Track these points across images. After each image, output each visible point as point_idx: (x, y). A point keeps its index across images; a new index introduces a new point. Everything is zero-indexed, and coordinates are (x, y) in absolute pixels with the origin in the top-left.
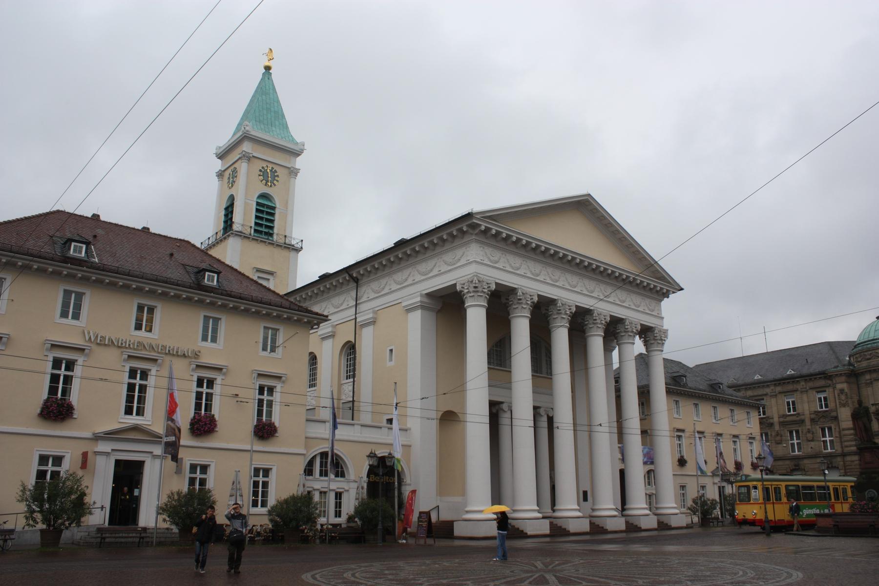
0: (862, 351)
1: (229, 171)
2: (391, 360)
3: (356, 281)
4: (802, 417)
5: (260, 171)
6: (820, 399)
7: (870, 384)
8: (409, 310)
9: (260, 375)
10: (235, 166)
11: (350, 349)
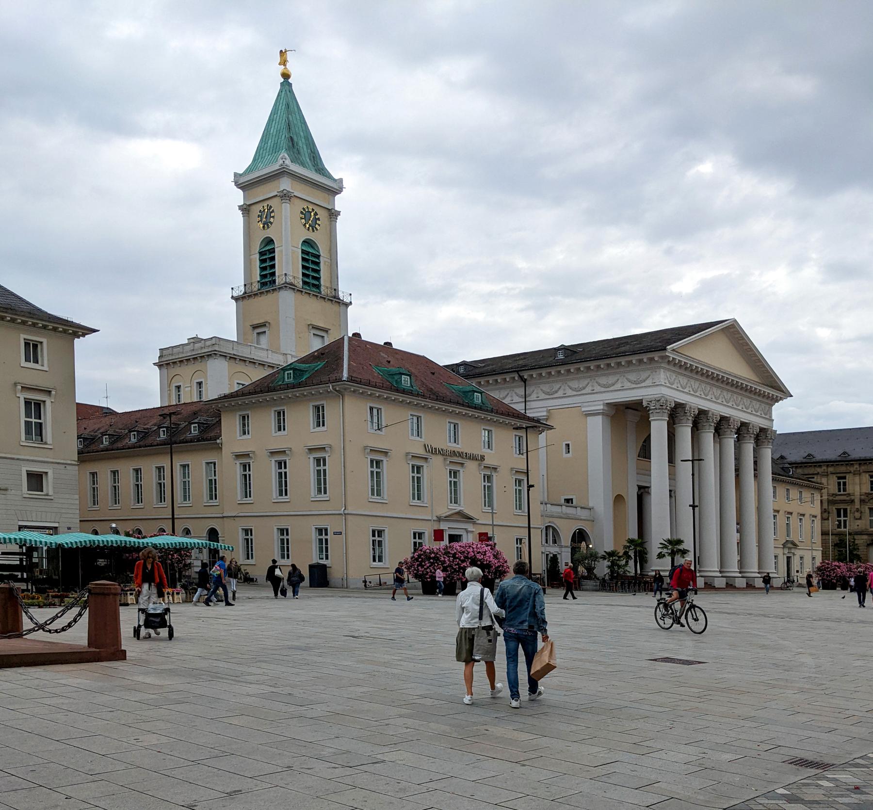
1: (259, 207)
3: (525, 381)
4: (852, 497)
5: (302, 213)
8: (589, 414)
10: (270, 203)
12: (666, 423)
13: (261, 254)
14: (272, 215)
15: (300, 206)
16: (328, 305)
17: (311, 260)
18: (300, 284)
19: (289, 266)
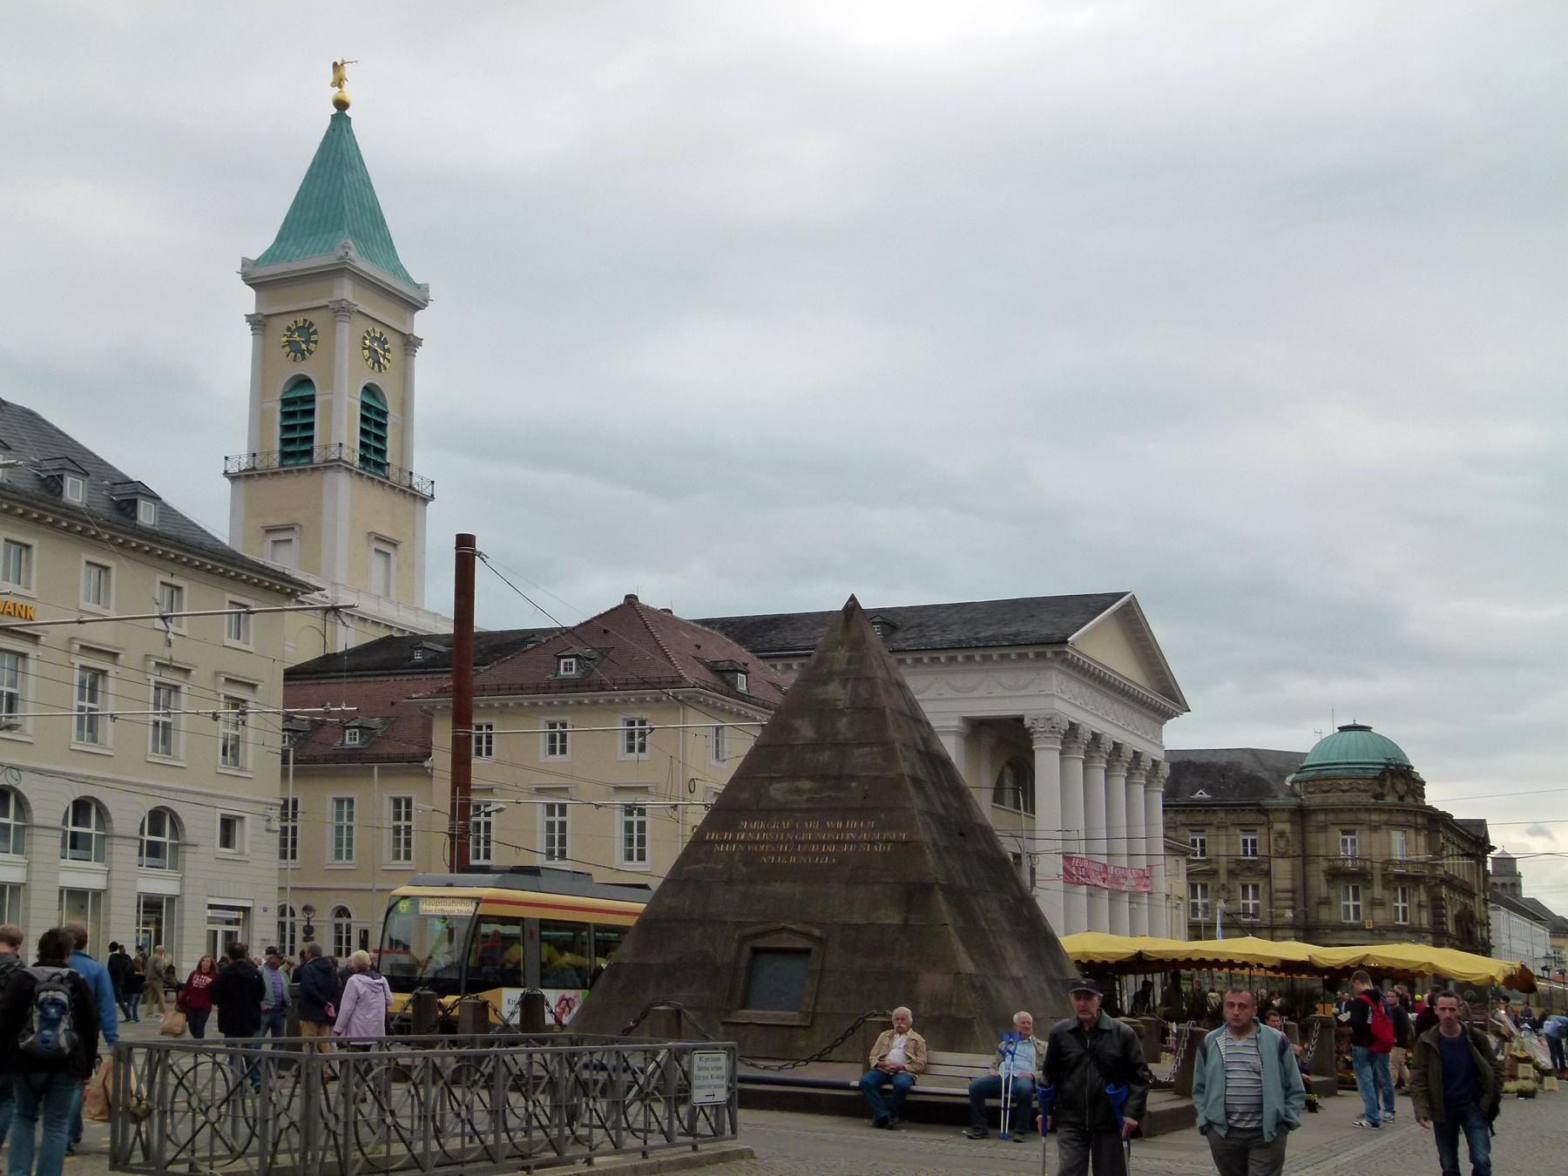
0: (1312, 780)
4: (1214, 866)
6: (1245, 842)
7: (1323, 828)
10: (311, 317)
13: (286, 402)
14: (313, 338)
16: (398, 499)
17: (374, 420)
19: (339, 428)
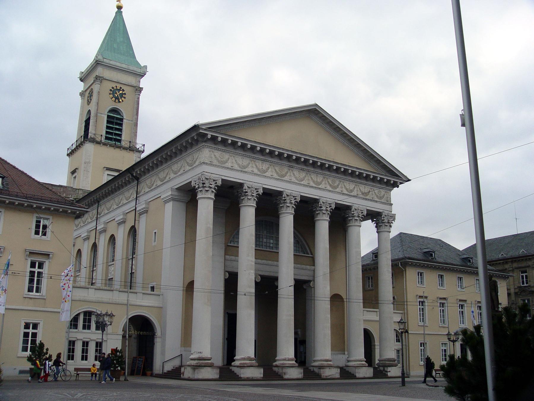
2: (155, 241)
5: (111, 90)
8: (166, 202)
9: (32, 253)
10: (92, 87)
11: (133, 231)
12: (211, 203)
15: (110, 86)
18: (103, 140)
